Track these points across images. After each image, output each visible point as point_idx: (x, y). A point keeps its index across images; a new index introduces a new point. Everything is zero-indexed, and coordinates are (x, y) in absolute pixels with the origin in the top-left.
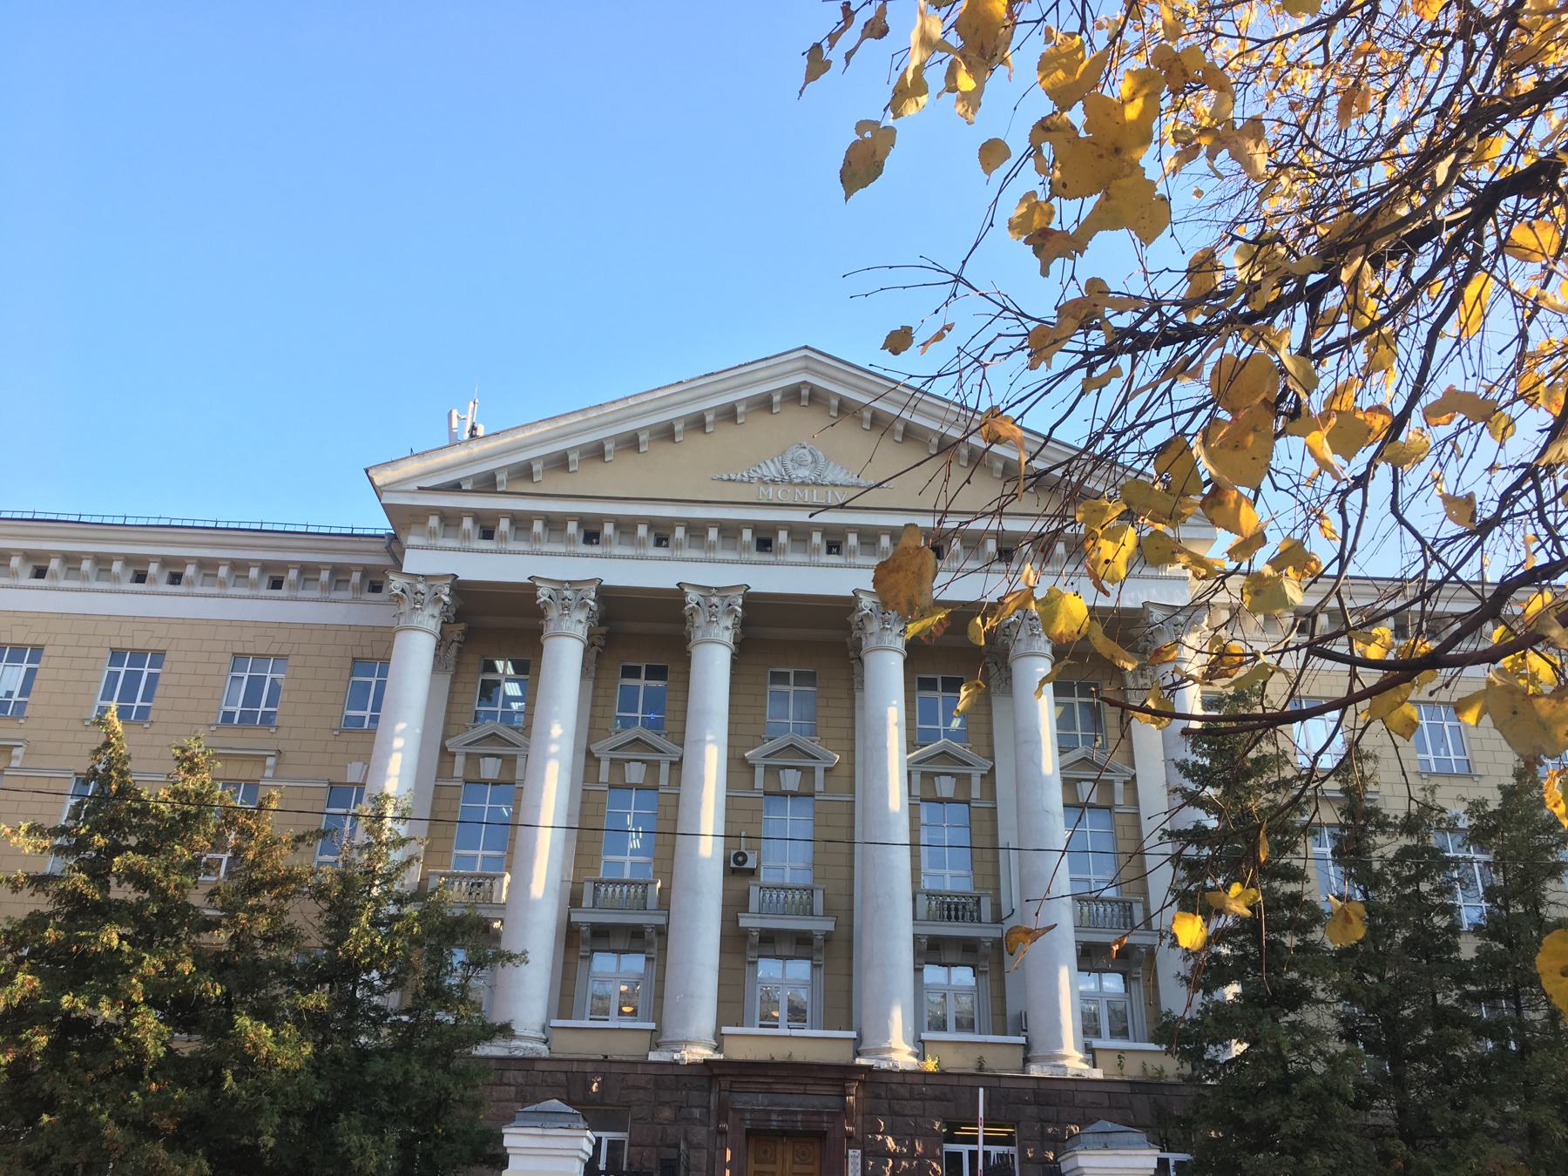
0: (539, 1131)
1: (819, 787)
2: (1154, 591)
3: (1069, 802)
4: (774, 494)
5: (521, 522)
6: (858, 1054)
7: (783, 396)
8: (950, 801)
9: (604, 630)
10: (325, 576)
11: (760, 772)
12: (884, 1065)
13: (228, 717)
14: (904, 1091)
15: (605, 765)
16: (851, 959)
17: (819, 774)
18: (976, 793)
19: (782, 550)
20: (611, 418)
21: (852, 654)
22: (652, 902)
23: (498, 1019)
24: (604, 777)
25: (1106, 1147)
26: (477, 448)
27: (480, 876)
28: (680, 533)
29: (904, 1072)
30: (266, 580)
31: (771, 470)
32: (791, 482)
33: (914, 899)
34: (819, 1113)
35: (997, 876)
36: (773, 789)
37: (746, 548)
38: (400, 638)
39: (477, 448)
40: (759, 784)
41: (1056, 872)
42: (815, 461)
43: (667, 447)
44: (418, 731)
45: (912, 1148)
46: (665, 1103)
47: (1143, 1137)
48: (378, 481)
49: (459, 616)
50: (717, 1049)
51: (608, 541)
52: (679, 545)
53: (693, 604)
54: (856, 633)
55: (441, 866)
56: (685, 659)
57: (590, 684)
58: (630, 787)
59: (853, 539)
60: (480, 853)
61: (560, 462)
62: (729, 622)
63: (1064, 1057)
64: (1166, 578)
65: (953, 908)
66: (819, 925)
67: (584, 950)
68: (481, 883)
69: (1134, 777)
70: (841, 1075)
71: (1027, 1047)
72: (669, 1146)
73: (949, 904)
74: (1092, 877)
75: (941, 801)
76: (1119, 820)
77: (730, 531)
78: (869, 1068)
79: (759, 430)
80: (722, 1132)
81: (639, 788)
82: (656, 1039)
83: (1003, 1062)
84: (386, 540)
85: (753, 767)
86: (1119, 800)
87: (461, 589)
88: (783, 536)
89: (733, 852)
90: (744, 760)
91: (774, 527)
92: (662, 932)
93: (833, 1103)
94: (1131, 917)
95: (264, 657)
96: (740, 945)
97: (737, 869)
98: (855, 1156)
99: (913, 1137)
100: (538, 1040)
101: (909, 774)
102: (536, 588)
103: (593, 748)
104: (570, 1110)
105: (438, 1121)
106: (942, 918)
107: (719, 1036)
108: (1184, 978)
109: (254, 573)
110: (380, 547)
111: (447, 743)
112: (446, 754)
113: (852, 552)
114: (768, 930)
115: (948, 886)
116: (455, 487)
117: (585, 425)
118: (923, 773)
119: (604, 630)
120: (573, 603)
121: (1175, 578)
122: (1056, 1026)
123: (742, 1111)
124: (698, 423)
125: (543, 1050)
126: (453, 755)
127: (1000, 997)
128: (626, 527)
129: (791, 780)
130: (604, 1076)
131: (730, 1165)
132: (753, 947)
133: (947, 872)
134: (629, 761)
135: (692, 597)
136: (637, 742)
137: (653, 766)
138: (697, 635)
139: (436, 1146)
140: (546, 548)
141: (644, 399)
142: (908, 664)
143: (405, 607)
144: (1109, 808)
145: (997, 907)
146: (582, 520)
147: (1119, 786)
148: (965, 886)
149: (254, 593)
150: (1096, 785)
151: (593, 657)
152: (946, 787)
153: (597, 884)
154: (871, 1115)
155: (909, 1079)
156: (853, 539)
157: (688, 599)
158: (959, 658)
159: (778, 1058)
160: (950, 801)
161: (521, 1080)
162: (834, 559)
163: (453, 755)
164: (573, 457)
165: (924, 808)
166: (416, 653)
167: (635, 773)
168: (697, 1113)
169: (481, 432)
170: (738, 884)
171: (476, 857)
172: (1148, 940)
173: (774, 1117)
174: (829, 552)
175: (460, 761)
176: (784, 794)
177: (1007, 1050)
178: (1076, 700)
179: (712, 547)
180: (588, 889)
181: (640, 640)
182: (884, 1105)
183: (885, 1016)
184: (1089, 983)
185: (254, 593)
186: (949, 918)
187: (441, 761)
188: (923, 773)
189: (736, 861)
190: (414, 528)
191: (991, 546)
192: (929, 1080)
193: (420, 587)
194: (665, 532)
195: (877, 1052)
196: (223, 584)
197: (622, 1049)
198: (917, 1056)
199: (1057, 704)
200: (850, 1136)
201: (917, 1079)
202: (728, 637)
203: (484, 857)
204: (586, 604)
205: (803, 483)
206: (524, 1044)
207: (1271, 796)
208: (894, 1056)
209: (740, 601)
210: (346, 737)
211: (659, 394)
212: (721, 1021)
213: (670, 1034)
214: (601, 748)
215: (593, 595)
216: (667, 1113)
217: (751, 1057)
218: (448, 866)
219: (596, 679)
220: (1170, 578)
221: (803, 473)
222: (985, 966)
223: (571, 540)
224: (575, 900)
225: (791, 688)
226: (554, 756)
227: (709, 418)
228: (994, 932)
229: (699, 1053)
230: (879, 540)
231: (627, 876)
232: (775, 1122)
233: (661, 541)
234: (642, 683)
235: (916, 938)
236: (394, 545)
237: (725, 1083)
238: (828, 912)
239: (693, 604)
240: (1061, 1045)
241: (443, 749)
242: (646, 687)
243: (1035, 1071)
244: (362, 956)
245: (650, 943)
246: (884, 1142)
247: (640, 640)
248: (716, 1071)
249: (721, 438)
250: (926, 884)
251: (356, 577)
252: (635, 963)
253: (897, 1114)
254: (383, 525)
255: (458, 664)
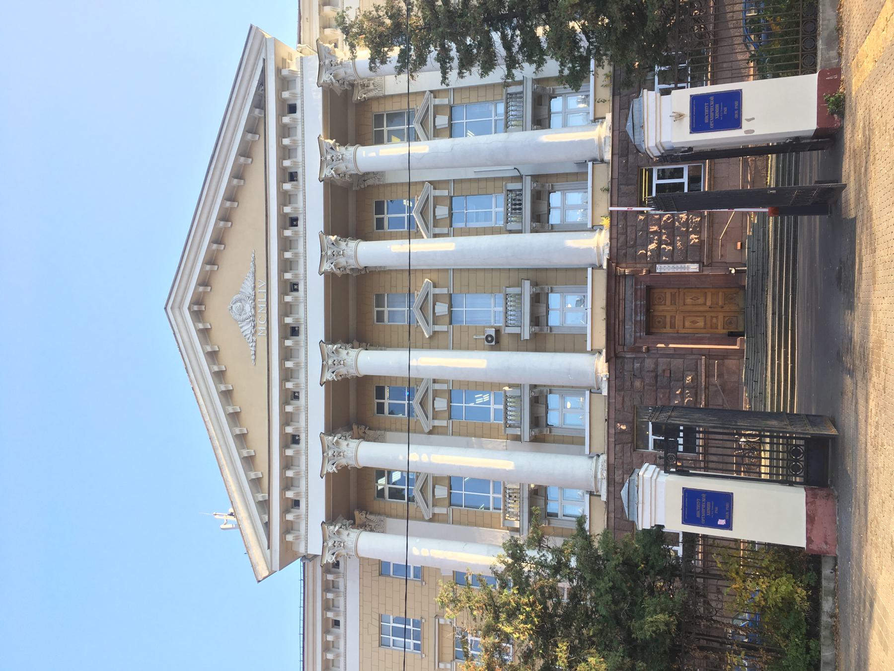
0: (640, 506)
1: (445, 291)
2: (310, 79)
3: (448, 133)
4: (262, 327)
5: (287, 484)
6: (601, 266)
7: (200, 322)
8: (451, 209)
9: (355, 427)
10: (330, 596)
11: (437, 328)
12: (607, 251)
13: (417, 647)
14: (622, 239)
15: (437, 423)
16: (547, 269)
17: (437, 291)
18: (445, 193)
19: (297, 320)
20: (219, 432)
21: (363, 272)
22: (517, 392)
23: (574, 526)
24: (444, 423)
25: (642, 127)
26: (242, 514)
27: (504, 496)
28: (289, 385)
29: (611, 239)
30: (335, 630)
31: (247, 328)
32: (254, 316)
33: (511, 232)
34: (636, 290)
35: (495, 179)
36: (447, 319)
37: (297, 343)
38: (361, 554)
39: (242, 514)
40: (444, 328)
41: (490, 143)
42: (240, 300)
43: (237, 395)
44: (418, 540)
45: (655, 232)
46: (632, 386)
47: (636, 100)
48: (267, 574)
49: (350, 517)
50: (600, 353)
51: (297, 429)
52: (297, 385)
53: (333, 375)
54: (348, 272)
55: (499, 518)
56: (366, 377)
57: (388, 434)
58: (450, 407)
59: (288, 276)
60: (491, 495)
61: (249, 461)
62: (343, 352)
63: (600, 138)
64: (302, 71)
65: (515, 206)
66: (527, 289)
67: (546, 431)
68: (509, 495)
69: (431, 92)
70: (613, 279)
71: (594, 161)
72: (657, 382)
73: (513, 209)
74: (493, 119)
75: (451, 215)
76: (458, 101)
77: (286, 354)
78: (608, 260)
79: (221, 337)
80: (648, 350)
81: (450, 401)
82: (594, 390)
83: (603, 176)
84: (306, 562)
85: (435, 332)
86: (445, 101)
87: (332, 518)
88: (288, 320)
89: (486, 343)
90: (430, 337)
91: (282, 326)
92: (533, 387)
93: (629, 282)
94: (516, 94)
95: (381, 628)
96: (541, 337)
97: (495, 341)
98: (661, 268)
99: (648, 233)
100: (597, 460)
101: (435, 236)
102: (328, 474)
103: (427, 430)
104: (626, 485)
105: (637, 566)
106: (521, 214)
107: (593, 352)
108: (537, 69)
109: (330, 638)
110: (311, 564)
111: (427, 518)
112: (434, 519)
113: (296, 275)
114: (531, 321)
115: (501, 209)
116: (267, 526)
117: (224, 447)
118: (434, 226)
119: (355, 427)
120: (336, 450)
121: (302, 66)
122: (582, 143)
123: (635, 338)
124: (220, 376)
125: (604, 458)
126: (434, 514)
127: (566, 176)
128: (287, 419)
129: (442, 309)
130: (616, 422)
131: (667, 344)
132: (541, 330)
133: (494, 210)
134: (434, 408)
135: (329, 376)
136: (422, 404)
137: (436, 394)
138: (353, 372)
139: (652, 568)
140: (303, 467)
141: (205, 411)
142: (366, 238)
143: (343, 552)
144: (451, 108)
145: (513, 179)
146: (284, 446)
147: (437, 101)
148: (501, 198)
149: (342, 637)
150: (439, 117)
151: (371, 433)
152: (442, 211)
153: (507, 425)
154: (636, 258)
155: (615, 235)
156: (288, 276)
157: (330, 379)
158: (357, 206)
159: (604, 316)
160: (451, 209)
161: (620, 472)
162: (301, 287)
163: (434, 514)
164: (245, 453)
165: (457, 225)
166: (371, 544)
167: (441, 404)
168: (637, 365)
169: (231, 510)
170: (505, 341)
171: (494, 498)
172: (529, 84)
173: (638, 318)
174: (297, 290)
175: (437, 510)
176: (451, 312)
177: (596, 173)
178: (385, 129)
179: (298, 364)
180: (510, 431)
181: (357, 407)
182: (630, 251)
183: (577, 250)
184: (556, 120)
185: (342, 637)
186: (520, 209)
187: (438, 521)
188: (434, 226)
189: (491, 341)
190: (295, 549)
191: (287, 186)
192: (615, 222)
193: (330, 544)
194: (290, 394)
195: (599, 255)
196: (338, 655)
197: (601, 411)
198: (601, 230)
199: (389, 140)
200: (649, 272)
201: (614, 231)
202: (353, 352)
203: (494, 493)
204: (337, 442)
205: (255, 308)
206: (600, 470)
207: (415, 9)
208: (601, 245)
209: (330, 346)
210: (426, 578)
211: (201, 401)
212: (583, 350)
213: (592, 382)
214: (426, 426)
215: (330, 438)
216: (637, 384)
217: (604, 332)
218: (500, 514)
219: (385, 430)
220: (302, 68)
221: (248, 308)
222: (548, 186)
223: (298, 452)
224: (517, 438)
225: (386, 310)
226: (429, 458)
227: (216, 368)
228: (528, 181)
229: (600, 366)
230: (287, 259)
231: (501, 407)
232: (641, 318)
233: (295, 396)
234: (387, 402)
235: (534, 231)
236: (307, 558)
237: (619, 349)
238: (519, 285)
239: (333, 375)
240: (593, 140)
241: (431, 520)
242: (390, 398)
243: (608, 156)
244: (532, 622)
245: (541, 392)
246: (651, 251)
247: (357, 407)
248: (612, 355)
249: (227, 360)
250: (501, 223)
251: (330, 577)
252: (553, 400)
253: (635, 242)
254: (297, 564)
255: (379, 514)
